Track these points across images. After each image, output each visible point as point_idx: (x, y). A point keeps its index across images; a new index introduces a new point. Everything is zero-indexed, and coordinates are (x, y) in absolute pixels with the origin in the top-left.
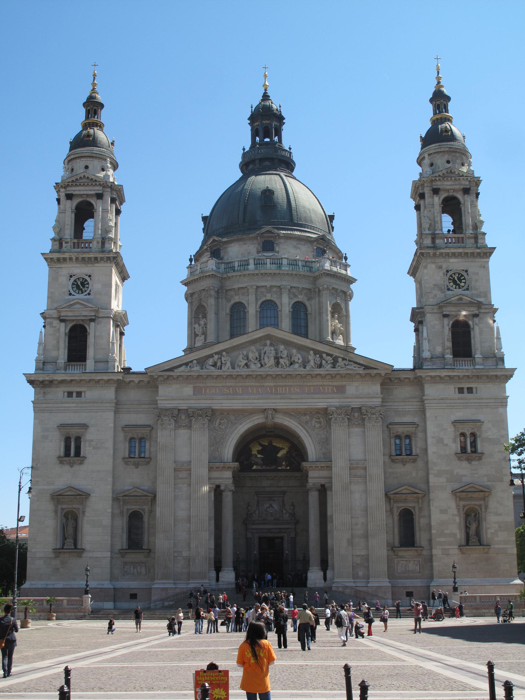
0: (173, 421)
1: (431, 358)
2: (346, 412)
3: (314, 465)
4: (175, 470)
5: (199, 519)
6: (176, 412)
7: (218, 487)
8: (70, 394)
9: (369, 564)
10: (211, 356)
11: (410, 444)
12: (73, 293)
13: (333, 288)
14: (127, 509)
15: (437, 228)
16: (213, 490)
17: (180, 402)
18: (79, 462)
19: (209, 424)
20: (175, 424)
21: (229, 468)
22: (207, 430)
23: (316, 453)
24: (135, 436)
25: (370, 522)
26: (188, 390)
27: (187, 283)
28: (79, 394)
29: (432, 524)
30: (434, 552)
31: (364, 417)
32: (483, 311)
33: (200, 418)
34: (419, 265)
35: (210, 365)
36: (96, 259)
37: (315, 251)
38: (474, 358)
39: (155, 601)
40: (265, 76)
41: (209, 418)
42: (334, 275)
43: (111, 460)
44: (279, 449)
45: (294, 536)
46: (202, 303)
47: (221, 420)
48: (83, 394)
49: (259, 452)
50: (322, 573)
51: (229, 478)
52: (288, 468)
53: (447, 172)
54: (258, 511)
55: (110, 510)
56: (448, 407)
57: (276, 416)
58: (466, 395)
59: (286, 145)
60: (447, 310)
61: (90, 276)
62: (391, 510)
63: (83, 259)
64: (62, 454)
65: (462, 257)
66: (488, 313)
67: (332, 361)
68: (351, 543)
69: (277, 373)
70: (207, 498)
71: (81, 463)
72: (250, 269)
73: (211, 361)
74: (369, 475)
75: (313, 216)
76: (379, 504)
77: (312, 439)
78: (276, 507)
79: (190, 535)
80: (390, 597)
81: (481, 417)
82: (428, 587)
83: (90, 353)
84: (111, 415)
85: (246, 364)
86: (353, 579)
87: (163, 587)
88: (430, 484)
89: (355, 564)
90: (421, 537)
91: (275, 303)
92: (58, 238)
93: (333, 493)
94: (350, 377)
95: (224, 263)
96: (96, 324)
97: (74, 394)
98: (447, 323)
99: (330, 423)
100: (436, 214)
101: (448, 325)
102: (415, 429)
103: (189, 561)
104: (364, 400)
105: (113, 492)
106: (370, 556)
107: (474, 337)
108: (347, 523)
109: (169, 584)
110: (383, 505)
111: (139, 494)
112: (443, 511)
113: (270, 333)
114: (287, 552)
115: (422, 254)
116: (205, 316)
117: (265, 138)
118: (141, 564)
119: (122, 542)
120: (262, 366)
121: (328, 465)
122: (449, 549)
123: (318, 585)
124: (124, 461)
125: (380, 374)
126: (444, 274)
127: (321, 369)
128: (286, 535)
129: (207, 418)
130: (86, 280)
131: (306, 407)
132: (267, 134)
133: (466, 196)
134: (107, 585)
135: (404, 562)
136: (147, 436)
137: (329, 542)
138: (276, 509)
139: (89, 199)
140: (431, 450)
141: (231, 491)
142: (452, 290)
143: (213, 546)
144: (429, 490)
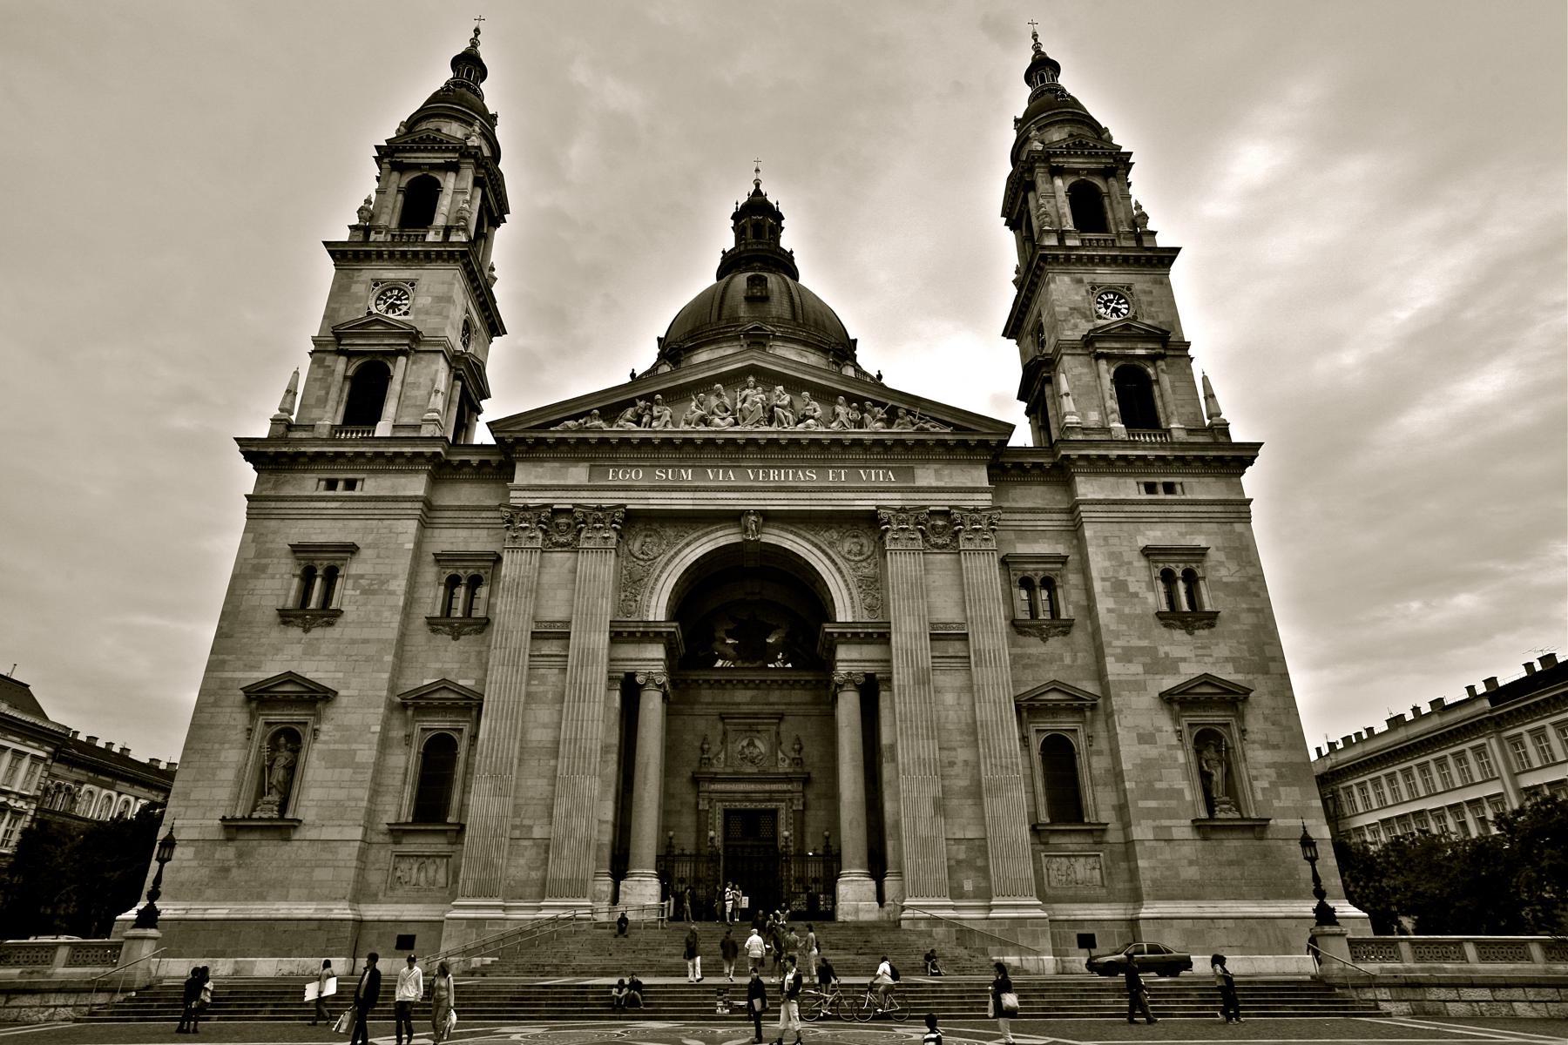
0: (540, 535)
1: (1083, 429)
2: (917, 518)
3: (849, 630)
4: (536, 636)
5: (580, 748)
6: (546, 513)
7: (631, 676)
8: (332, 485)
9: (987, 859)
11: (1053, 600)
12: (375, 311)
14: (423, 729)
15: (1064, 223)
16: (619, 687)
17: (559, 494)
18: (325, 619)
19: (618, 542)
20: (544, 540)
22: (613, 551)
23: (853, 607)
24: (461, 572)
25: (985, 758)
26: (578, 474)
28: (350, 485)
29: (1124, 768)
30: (1137, 833)
31: (957, 528)
32: (1171, 353)
33: (598, 525)
34: (1033, 292)
35: (629, 421)
36: (427, 255)
38: (1169, 431)
39: (448, 955)
40: (757, 170)
41: (618, 527)
43: (398, 618)
45: (801, 808)
47: (646, 536)
48: (359, 484)
50: (872, 885)
51: (661, 660)
52: (789, 665)
53: (1074, 143)
54: (723, 753)
55: (378, 728)
56: (1130, 520)
57: (766, 530)
58: (1161, 496)
60: (1103, 347)
61: (412, 285)
62: (1024, 739)
63: (404, 253)
64: (290, 604)
65: (1118, 265)
66: (1181, 356)
67: (885, 416)
68: (940, 807)
69: (770, 436)
70: (602, 699)
71: (330, 624)
73: (629, 413)
74: (974, 651)
75: (827, 323)
76: (1001, 717)
77: (843, 577)
78: (761, 747)
79: (554, 786)
80: (1049, 947)
81: (1200, 541)
82: (1134, 922)
83: (390, 408)
84: (412, 526)
85: (703, 420)
86: (952, 898)
87: (473, 916)
88: (1110, 678)
89: (953, 863)
90: (1099, 803)
92: (362, 224)
93: (896, 691)
94: (923, 450)
96: (410, 362)
97: (341, 485)
98: (1106, 371)
99: (884, 543)
100: (1059, 205)
101: (1108, 371)
102: (1060, 566)
103: (547, 852)
104: (954, 496)
105: (392, 688)
106: (989, 841)
107: (1162, 396)
108: (929, 759)
109: (487, 910)
110: (1012, 718)
111: (452, 696)
112: (1145, 738)
113: (755, 362)
114: (786, 833)
115: (1044, 258)
118: (438, 861)
119: (398, 805)
120: (737, 423)
121: (882, 630)
122: (1170, 827)
123: (865, 917)
124: (429, 624)
125: (983, 444)
126: (1087, 291)
130: (405, 293)
131: (830, 508)
133: (1112, 181)
134: (341, 911)
135: (1063, 859)
136: (486, 573)
137: (888, 807)
138: (763, 750)
139: (431, 174)
140: (1104, 604)
141: (659, 686)
142: (1105, 319)
144: (1106, 695)
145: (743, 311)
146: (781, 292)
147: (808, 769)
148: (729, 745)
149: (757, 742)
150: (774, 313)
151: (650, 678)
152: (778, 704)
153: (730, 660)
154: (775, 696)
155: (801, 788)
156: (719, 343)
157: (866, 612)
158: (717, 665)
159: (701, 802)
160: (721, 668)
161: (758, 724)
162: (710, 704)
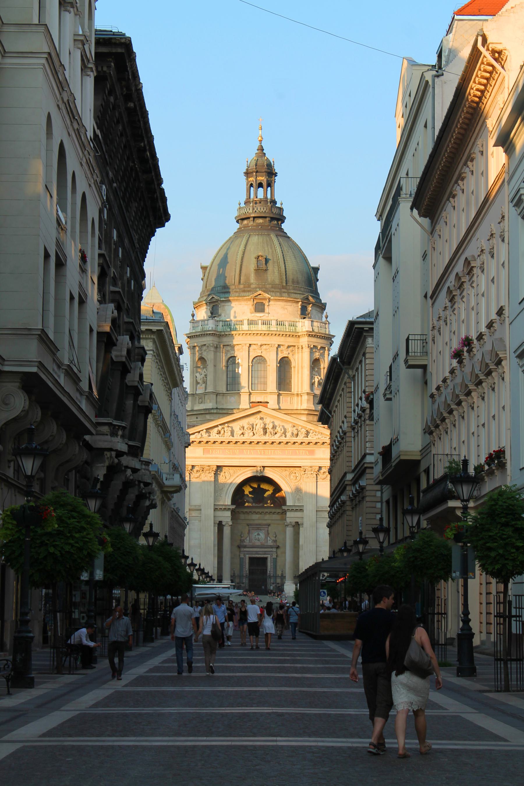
10: (217, 426)
13: (314, 346)
16: (217, 525)
21: (228, 509)
27: (190, 336)
37: (299, 310)
41: (215, 472)
42: (315, 335)
44: (266, 491)
45: (275, 557)
46: (203, 356)
49: (250, 492)
52: (272, 505)
59: (277, 198)
72: (244, 329)
73: (216, 430)
85: (243, 434)
91: (265, 359)
95: (222, 321)
116: (205, 367)
117: (258, 188)
127: (297, 438)
128: (269, 556)
129: (213, 472)
132: (260, 185)
143: (216, 565)
145: (252, 279)
146: (274, 262)
147: (278, 544)
148: (250, 535)
149: (260, 533)
150: (269, 280)
151: (227, 523)
152: (269, 520)
153: (250, 503)
154: (267, 517)
155: (275, 550)
156: (240, 301)
157: (297, 501)
158: (245, 505)
159: (241, 555)
160: (248, 507)
161: (259, 527)
162: (242, 520)
